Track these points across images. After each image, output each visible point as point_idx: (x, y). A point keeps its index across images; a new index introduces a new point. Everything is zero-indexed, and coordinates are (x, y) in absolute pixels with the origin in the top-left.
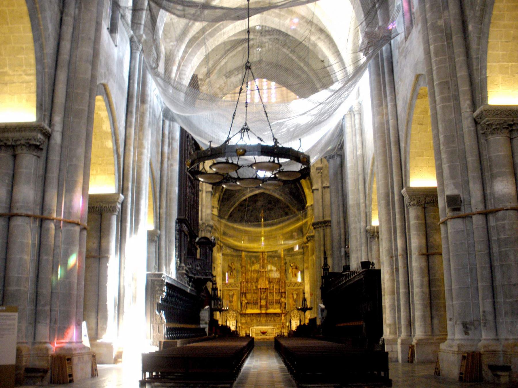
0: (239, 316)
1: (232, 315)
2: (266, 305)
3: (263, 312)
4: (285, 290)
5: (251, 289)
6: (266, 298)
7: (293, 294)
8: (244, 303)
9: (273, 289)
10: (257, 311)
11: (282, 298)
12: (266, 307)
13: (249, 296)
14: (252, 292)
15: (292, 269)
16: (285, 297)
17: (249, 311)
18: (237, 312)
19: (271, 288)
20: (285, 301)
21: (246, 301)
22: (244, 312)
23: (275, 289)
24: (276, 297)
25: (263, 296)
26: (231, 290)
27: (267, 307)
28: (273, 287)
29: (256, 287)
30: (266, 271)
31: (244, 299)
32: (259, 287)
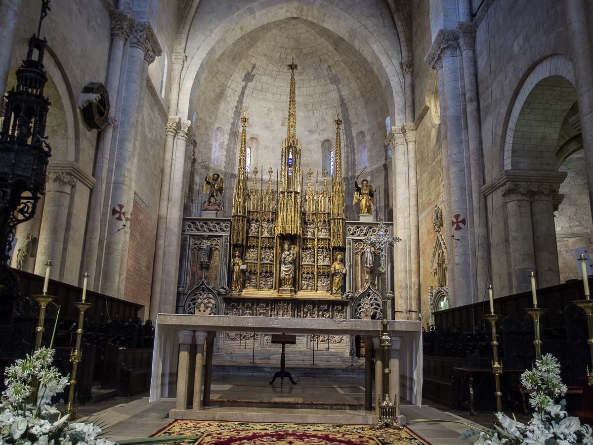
0: (223, 306)
1: (206, 301)
2: (294, 278)
3: (287, 295)
4: (344, 242)
5: (258, 238)
6: (294, 262)
7: (363, 254)
8: (236, 268)
9: (314, 240)
10: (273, 294)
11: (336, 263)
12: (294, 285)
13: (251, 255)
14: (260, 245)
15: (361, 194)
16: (343, 261)
17: (250, 292)
18: (219, 294)
19: (309, 236)
20: (344, 272)
21: (244, 267)
22: (235, 293)
23: (318, 240)
24: (323, 261)
25: (290, 253)
26: (209, 238)
27: (296, 284)
28: (314, 235)
29: (270, 231)
30: (297, 193)
31: (236, 260)
32: (278, 231)
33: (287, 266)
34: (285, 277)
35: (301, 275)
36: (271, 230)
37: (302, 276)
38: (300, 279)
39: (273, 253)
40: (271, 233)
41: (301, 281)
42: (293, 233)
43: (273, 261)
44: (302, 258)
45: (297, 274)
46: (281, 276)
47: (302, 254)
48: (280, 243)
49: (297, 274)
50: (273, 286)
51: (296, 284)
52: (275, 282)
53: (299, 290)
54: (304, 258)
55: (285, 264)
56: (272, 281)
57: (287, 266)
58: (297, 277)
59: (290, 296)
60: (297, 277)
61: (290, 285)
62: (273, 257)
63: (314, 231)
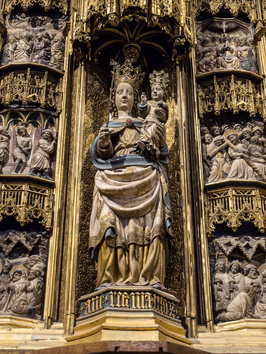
33: (125, 171)
34: (114, 230)
35: (210, 240)
36: (48, 45)
37: (212, 249)
38: (205, 260)
39: (51, 138)
40: (47, 57)
41: (213, 272)
42: (155, 10)
43: (51, 173)
44: (208, 160)
45: (188, 227)
46: (94, 231)
47: (203, 141)
48: (88, 87)
49: (188, 227)
50: (41, 300)
51: (183, 284)
52: (60, 278)
53: (201, 321)
54: (219, 158)
55: (118, 164)
56: (42, 276)
57: (125, 171)
58: (189, 244)
59: (154, 336)
60: (189, 244)
61: (149, 274)
62: (52, 156)
63: (250, 52)
